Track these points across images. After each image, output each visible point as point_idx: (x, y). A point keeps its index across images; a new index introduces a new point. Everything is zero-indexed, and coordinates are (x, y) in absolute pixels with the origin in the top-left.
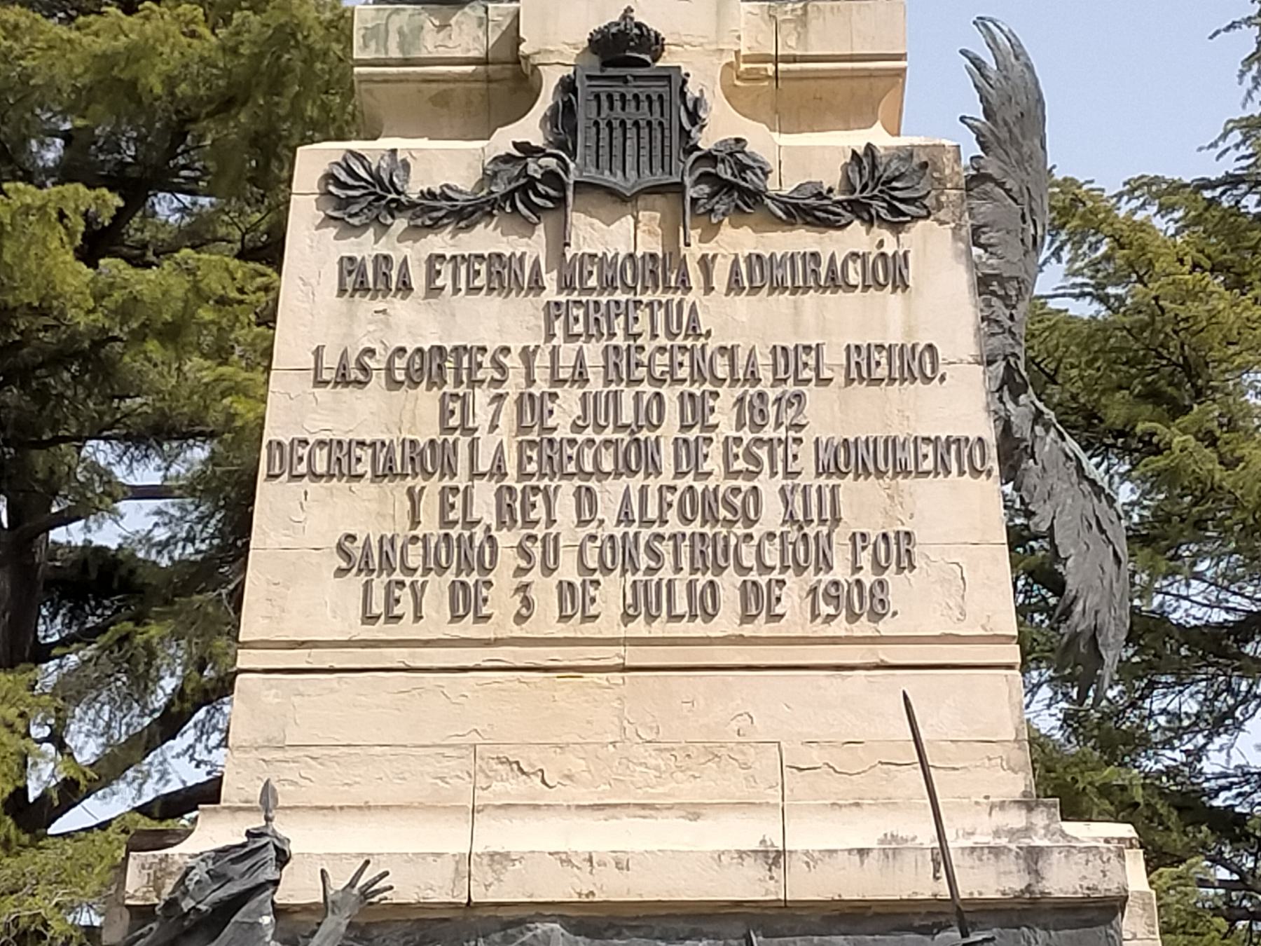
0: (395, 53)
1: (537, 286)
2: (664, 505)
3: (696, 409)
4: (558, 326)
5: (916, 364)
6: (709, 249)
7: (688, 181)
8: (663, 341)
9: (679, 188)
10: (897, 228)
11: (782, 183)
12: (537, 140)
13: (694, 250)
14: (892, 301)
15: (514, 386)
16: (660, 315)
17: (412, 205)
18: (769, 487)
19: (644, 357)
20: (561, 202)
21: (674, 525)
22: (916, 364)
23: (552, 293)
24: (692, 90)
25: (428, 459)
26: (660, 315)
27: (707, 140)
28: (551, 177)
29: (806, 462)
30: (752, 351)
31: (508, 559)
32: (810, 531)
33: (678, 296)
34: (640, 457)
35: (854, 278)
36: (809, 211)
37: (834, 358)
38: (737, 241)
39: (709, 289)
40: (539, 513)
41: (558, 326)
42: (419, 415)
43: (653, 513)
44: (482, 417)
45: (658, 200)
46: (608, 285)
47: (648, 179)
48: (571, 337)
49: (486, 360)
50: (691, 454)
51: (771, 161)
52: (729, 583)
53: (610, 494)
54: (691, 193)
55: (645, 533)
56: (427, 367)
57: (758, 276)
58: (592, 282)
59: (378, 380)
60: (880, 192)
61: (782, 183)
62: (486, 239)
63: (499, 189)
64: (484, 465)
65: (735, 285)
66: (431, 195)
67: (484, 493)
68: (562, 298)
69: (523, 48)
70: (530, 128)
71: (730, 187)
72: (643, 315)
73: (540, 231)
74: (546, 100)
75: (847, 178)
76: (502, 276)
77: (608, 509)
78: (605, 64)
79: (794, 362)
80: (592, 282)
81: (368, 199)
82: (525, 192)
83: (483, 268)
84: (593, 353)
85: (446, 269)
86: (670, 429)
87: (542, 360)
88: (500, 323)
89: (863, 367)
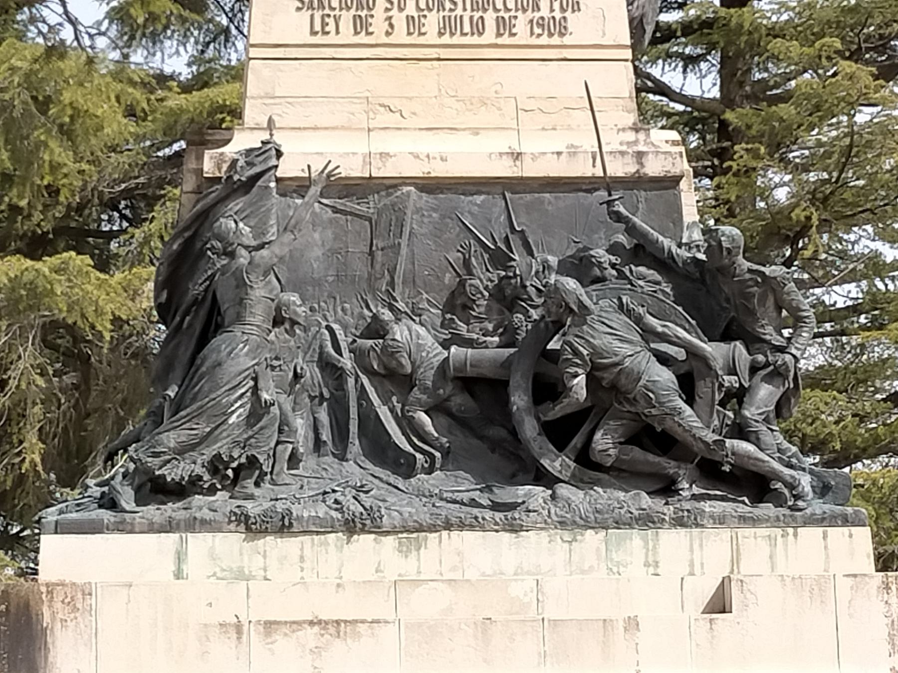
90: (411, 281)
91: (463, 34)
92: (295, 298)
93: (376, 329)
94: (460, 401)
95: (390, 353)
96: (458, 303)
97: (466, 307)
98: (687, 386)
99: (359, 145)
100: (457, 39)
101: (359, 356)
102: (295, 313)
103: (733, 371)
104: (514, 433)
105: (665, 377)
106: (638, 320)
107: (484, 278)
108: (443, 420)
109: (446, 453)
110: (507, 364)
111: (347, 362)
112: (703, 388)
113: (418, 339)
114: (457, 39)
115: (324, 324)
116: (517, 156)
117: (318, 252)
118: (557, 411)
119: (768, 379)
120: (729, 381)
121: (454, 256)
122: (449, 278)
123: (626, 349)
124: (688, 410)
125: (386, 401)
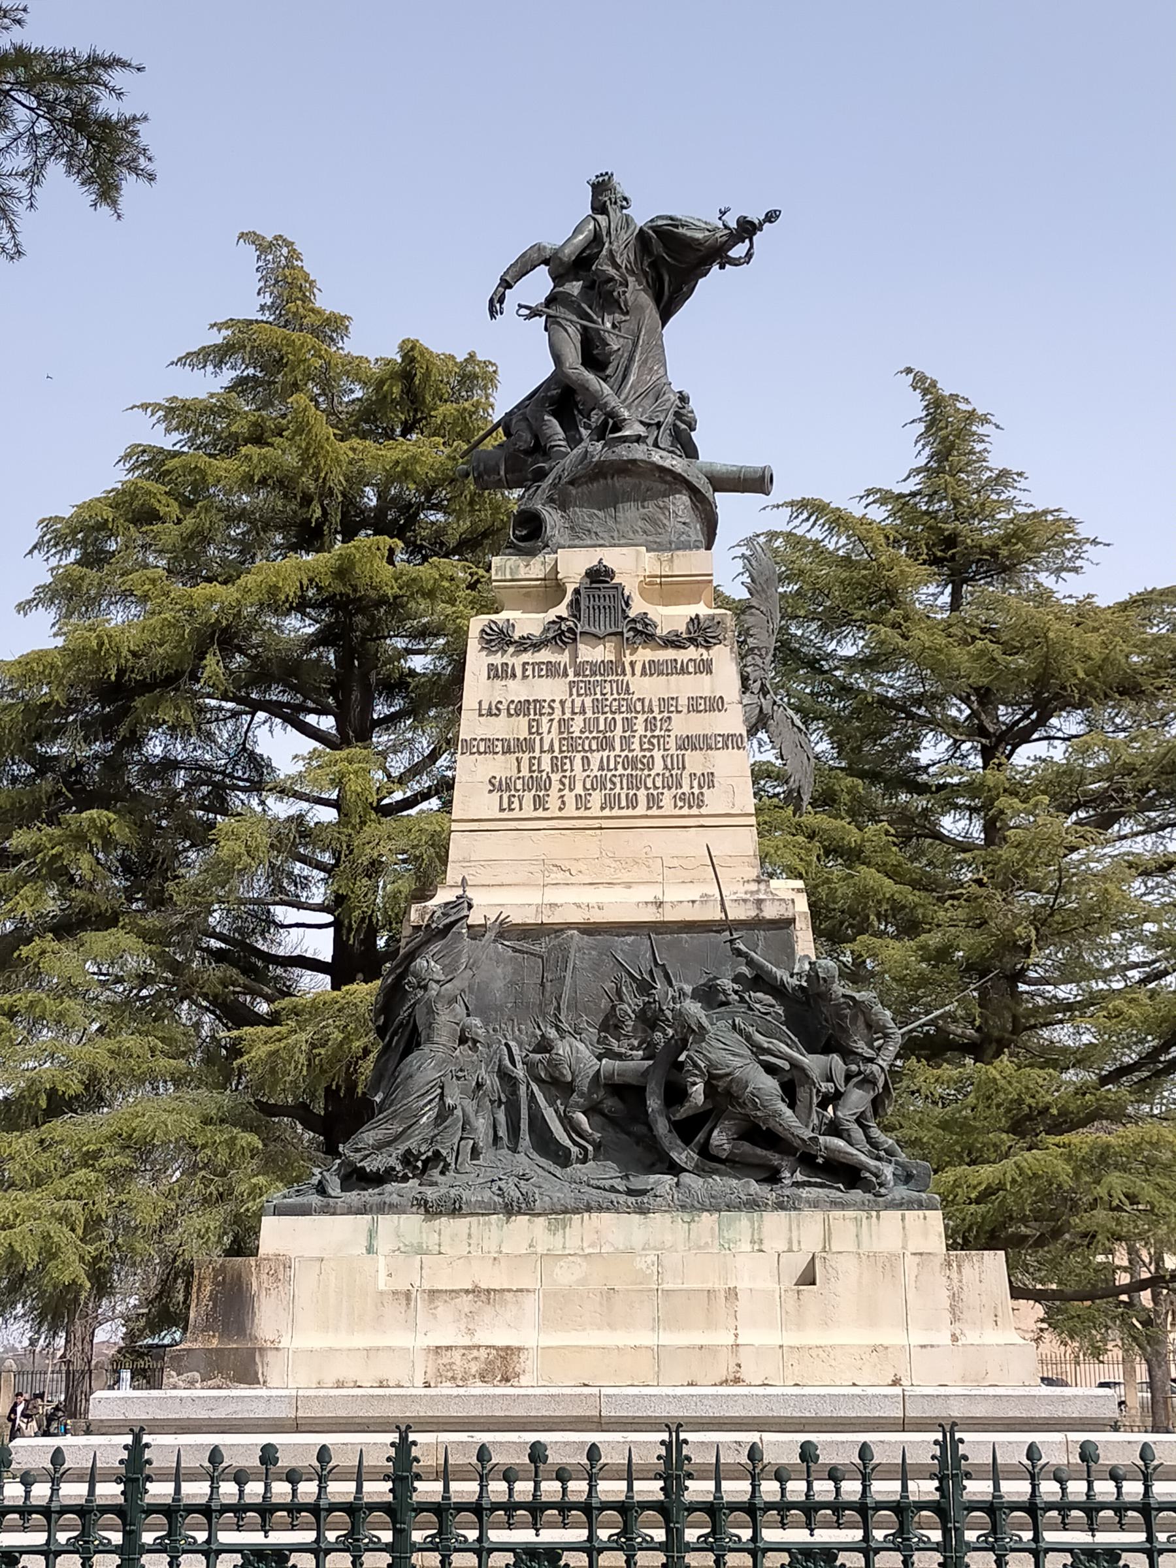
0: (508, 577)
1: (566, 675)
2: (616, 763)
3: (629, 724)
4: (574, 690)
5: (716, 704)
6: (633, 658)
7: (625, 630)
8: (615, 696)
9: (622, 634)
10: (708, 648)
11: (662, 631)
12: (565, 615)
13: (627, 659)
14: (705, 677)
15: (557, 715)
16: (614, 685)
17: (516, 642)
18: (658, 755)
19: (608, 703)
20: (575, 640)
21: (620, 771)
22: (716, 704)
23: (571, 677)
24: (626, 593)
25: (525, 745)
26: (614, 685)
27: (632, 614)
28: (570, 630)
29: (672, 745)
30: (651, 701)
31: (556, 785)
32: (674, 772)
33: (621, 678)
34: (606, 744)
35: (691, 669)
36: (672, 642)
37: (683, 702)
38: (645, 654)
39: (633, 674)
40: (567, 767)
41: (574, 690)
42: (520, 727)
43: (612, 766)
44: (545, 729)
45: (613, 638)
46: (594, 674)
47: (609, 630)
48: (579, 695)
49: (546, 705)
50: (626, 742)
51: (657, 620)
52: (642, 794)
53: (595, 758)
54: (626, 635)
55: (609, 774)
56: (522, 708)
57: (653, 669)
58: (588, 672)
59: (504, 713)
60: (700, 634)
61: (662, 631)
62: (545, 655)
63: (550, 635)
64: (546, 747)
65: (644, 673)
66: (523, 638)
67: (546, 758)
68: (576, 679)
69: (559, 576)
70: (562, 610)
71: (642, 633)
72: (608, 685)
73: (567, 651)
74: (568, 597)
75: (688, 628)
76: (552, 670)
77: (595, 765)
78: (592, 582)
79: (669, 704)
80: (588, 672)
81: (498, 639)
82: (561, 636)
83: (544, 667)
84: (588, 701)
85: (530, 668)
86: (619, 732)
87: (568, 704)
88: (551, 689)
89: (694, 706)
90: (573, 1006)
91: (620, 808)
92: (476, 1021)
93: (544, 1046)
94: (610, 1104)
95: (554, 1065)
96: (611, 1025)
97: (617, 1027)
98: (790, 1092)
99: (534, 897)
100: (616, 812)
101: (530, 1066)
102: (477, 1034)
103: (830, 1079)
104: (651, 1129)
105: (770, 1084)
106: (748, 1038)
107: (631, 1004)
108: (598, 1119)
109: (597, 1147)
110: (645, 1073)
111: (520, 1072)
112: (802, 1093)
113: (579, 1054)
114: (616, 812)
115: (503, 1041)
116: (659, 904)
117: (500, 984)
118: (682, 1113)
119: (859, 1085)
120: (826, 1087)
121: (609, 986)
122: (604, 1003)
123: (737, 1062)
124: (788, 1112)
125: (551, 1103)
